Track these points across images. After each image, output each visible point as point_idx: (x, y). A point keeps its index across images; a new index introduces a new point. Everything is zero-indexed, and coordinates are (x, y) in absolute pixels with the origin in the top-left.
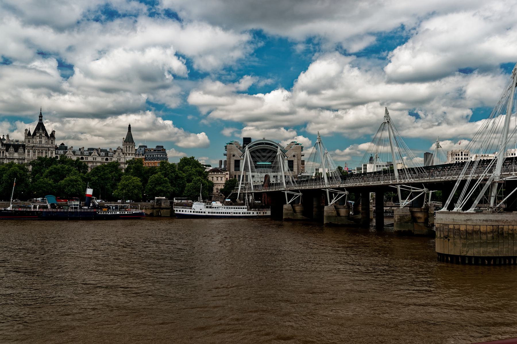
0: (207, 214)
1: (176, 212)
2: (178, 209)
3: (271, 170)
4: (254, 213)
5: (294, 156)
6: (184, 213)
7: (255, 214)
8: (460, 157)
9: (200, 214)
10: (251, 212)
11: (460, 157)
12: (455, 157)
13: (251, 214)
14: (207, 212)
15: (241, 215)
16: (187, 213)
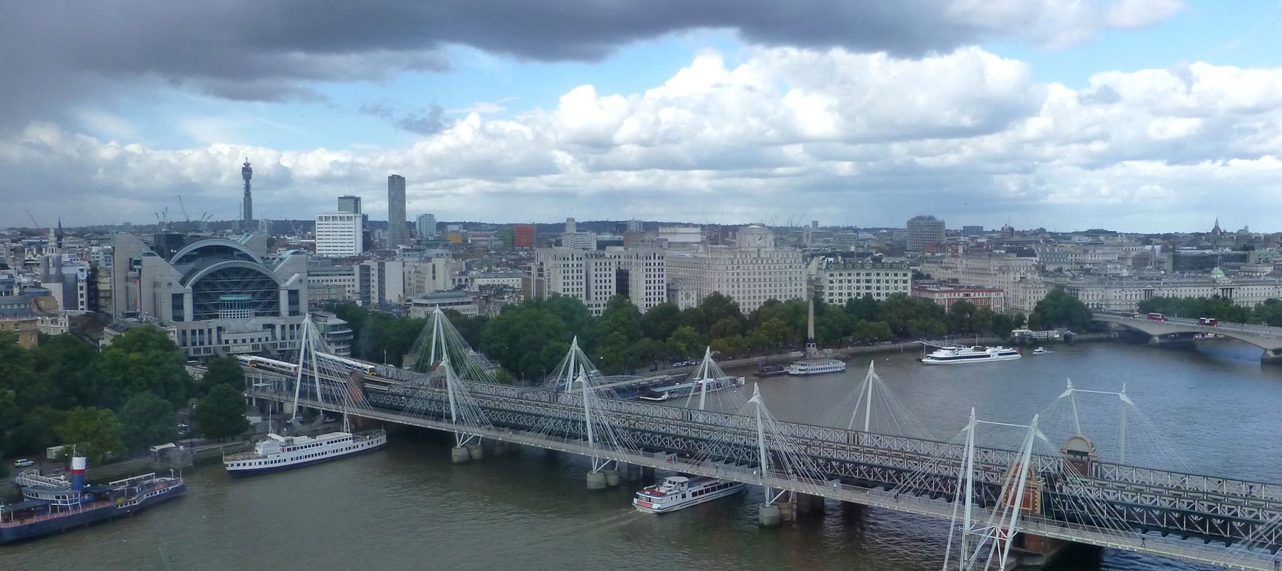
0: (289, 462)
1: (229, 468)
2: (235, 463)
3: (253, 311)
4: (363, 445)
5: (301, 281)
6: (247, 467)
7: (366, 447)
8: (570, 262)
9: (278, 465)
10: (360, 443)
11: (570, 262)
12: (562, 263)
13: (360, 449)
14: (288, 458)
15: (345, 452)
16: (253, 467)
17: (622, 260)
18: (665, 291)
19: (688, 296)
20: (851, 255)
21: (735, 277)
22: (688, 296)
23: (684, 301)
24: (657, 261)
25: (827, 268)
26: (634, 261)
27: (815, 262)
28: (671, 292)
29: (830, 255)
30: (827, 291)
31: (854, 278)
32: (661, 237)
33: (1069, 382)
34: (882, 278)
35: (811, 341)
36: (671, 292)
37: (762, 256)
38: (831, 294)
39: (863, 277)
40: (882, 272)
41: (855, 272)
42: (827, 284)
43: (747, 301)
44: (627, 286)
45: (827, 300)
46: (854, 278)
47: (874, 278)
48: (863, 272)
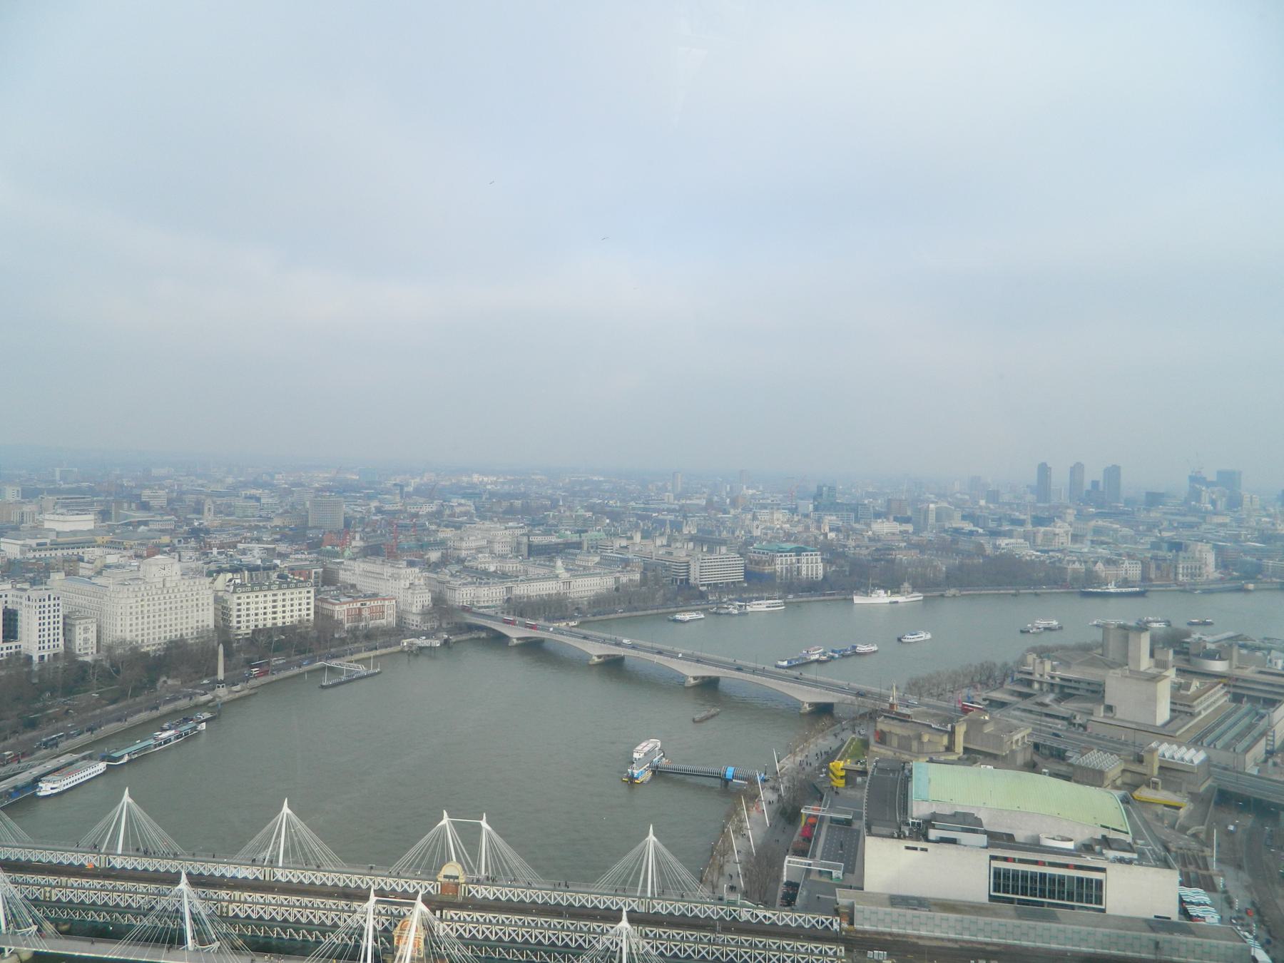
17: (9, 599)
18: (61, 631)
19: (86, 630)
20: (257, 568)
21: (139, 610)
22: (86, 630)
23: (83, 636)
24: (52, 602)
25: (234, 592)
26: (25, 602)
27: (223, 579)
28: (68, 629)
29: (235, 570)
30: (235, 613)
31: (261, 599)
32: (47, 525)
33: (445, 813)
34: (288, 597)
35: (221, 682)
36: (68, 629)
37: (168, 585)
38: (239, 616)
39: (270, 598)
40: (288, 592)
41: (262, 594)
42: (235, 607)
43: (151, 631)
44: (16, 626)
45: (234, 624)
46: (261, 599)
47: (280, 597)
48: (269, 593)
